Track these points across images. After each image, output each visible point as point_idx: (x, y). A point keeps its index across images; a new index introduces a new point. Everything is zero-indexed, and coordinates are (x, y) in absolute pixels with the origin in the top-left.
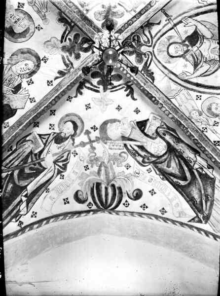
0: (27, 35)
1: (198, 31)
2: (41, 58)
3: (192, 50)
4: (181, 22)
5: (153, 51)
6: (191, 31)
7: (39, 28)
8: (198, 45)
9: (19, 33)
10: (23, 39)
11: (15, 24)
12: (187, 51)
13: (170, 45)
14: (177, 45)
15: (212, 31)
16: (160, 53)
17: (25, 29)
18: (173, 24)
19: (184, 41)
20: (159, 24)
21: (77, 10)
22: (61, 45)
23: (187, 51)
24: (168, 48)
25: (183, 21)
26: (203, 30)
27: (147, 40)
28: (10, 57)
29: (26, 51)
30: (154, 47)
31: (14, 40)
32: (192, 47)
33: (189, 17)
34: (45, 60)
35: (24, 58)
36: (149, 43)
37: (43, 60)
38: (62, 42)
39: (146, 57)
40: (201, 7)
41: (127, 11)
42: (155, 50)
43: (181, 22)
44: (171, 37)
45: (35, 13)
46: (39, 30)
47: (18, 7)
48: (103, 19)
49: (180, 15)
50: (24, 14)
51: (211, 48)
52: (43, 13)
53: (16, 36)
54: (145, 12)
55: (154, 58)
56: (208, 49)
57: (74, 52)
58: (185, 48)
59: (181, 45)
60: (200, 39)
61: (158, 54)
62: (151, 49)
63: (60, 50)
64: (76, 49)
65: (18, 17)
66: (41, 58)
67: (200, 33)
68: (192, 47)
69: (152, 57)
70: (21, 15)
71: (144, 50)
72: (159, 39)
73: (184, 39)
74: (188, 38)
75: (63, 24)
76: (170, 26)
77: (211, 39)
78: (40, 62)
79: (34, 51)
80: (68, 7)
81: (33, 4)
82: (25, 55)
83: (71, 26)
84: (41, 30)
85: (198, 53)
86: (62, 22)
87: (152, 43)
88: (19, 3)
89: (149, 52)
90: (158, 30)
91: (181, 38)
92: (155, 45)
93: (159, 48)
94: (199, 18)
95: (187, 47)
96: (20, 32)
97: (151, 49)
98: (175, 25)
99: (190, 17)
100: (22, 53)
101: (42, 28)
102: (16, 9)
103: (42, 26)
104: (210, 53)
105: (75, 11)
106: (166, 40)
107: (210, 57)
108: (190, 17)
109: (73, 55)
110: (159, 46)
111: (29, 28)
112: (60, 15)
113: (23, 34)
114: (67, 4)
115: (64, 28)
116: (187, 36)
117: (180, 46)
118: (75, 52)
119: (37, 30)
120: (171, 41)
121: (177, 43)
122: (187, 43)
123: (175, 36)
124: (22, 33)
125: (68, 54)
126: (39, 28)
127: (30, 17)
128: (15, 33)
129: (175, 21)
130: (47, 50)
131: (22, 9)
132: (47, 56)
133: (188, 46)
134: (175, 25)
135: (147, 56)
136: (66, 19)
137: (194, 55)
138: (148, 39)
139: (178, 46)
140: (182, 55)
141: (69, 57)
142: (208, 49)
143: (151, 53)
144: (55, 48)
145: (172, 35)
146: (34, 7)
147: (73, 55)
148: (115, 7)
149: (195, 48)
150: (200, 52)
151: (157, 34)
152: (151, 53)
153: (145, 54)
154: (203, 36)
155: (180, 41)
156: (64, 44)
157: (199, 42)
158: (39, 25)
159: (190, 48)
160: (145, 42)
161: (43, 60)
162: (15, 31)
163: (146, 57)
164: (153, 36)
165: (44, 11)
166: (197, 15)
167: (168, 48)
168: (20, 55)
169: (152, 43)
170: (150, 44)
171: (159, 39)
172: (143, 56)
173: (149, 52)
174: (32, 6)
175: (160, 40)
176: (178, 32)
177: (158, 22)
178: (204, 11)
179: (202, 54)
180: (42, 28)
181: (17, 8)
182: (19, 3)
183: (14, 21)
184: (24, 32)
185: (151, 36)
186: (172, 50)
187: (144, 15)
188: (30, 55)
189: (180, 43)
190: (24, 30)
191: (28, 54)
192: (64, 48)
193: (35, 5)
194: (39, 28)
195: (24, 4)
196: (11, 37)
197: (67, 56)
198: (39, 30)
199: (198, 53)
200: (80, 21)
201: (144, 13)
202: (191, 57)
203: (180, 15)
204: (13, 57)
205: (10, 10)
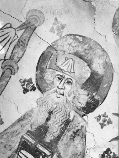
11: (74, 81)
47: (34, 89)
52: (20, 33)
65: (57, 83)
70: (49, 76)
81: (14, 64)
88: (25, 91)
102: (42, 92)
127: (43, 58)
131: (34, 81)
146: (16, 59)
162: (89, 76)
165: (12, 32)
174: (16, 63)
181: (37, 90)
182: (25, 91)
183: (68, 87)
190: (78, 60)
193: (11, 58)
195: (23, 82)
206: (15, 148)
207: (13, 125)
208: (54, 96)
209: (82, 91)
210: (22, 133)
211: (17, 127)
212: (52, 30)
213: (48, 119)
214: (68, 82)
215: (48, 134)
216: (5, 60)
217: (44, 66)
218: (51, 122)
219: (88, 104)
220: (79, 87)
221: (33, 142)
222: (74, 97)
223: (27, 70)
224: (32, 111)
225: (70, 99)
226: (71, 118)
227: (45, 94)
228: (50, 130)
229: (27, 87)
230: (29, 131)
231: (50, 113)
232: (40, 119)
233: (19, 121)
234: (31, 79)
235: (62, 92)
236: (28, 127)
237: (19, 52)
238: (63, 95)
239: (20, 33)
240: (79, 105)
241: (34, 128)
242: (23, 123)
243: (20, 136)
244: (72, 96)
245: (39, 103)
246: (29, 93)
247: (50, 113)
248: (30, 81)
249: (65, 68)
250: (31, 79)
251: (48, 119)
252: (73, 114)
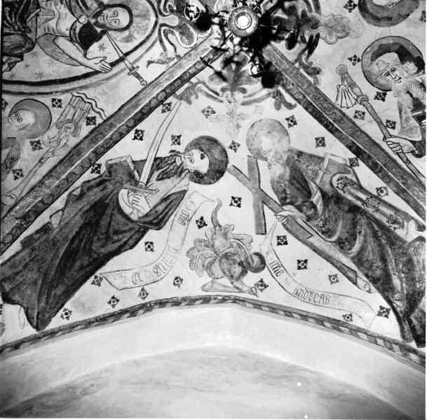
0: (376, 48)
1: (80, 48)
2: (357, 8)
3: (88, 17)
4: (113, 65)
5: (157, 16)
6: (94, 48)
7: (355, 59)
8: (79, 26)
9: (389, 52)
10: (384, 42)
12: (96, 15)
13: (127, 27)
14: (115, 25)
15: (58, 50)
16: (144, 13)
17: (379, 59)
18: (126, 62)
19: (104, 32)
20: (150, 63)
21: (288, 88)
22: (320, 28)
23: (96, 15)
24: (131, 22)
25: (109, 66)
26: (73, 50)
27: (170, 36)
28: (412, 12)
29: (383, 23)
30: (156, 23)
31: (403, 43)
32: (89, 22)
33: (100, 72)
34: (350, 5)
35: (387, 10)
36: (164, 31)
37: (355, 6)
38: (318, 36)
39: (169, 6)
40: (81, 88)
41: (204, 84)
42: (153, 19)
43: (113, 65)
44: (128, 39)
45: (358, 84)
46: (355, 56)
47: (385, 94)
48: (244, 71)
49: (116, 75)
50: (377, 83)
51: (54, 21)
52: (346, 83)
53: (397, 47)
54: (174, 81)
55: (156, 4)
56: (59, 18)
57: (297, 17)
58: (100, 20)
59: (108, 25)
60: (77, 36)
61: (148, 11)
62: (161, 20)
63: (321, 22)
64: (295, 22)
66: (357, 8)
67: (77, 45)
68: (89, 22)
69: (158, 6)
70: (382, 81)
71: (174, 19)
72: (148, 37)
73: (105, 38)
74: (97, 37)
75: (313, 66)
76: (131, 58)
77: (57, 36)
78: (359, 4)
79: (368, 22)
80: (303, 92)
82: (385, 15)
83: (300, 63)
84: (351, 55)
85: (78, 12)
86: (314, 69)
87: (160, 30)
88: (383, 100)
89: (164, 16)
90: (149, 53)
91: (109, 37)
92: (154, 28)
93: (147, 21)
94: (83, 70)
95: (97, 22)
96: (388, 54)
97: (161, 20)
98: (121, 60)
99: (97, 72)
100: (390, 19)
101: (350, 59)
102: (390, 90)
103: (349, 63)
104: (56, 12)
105: (291, 86)
106: (136, 35)
107: (56, 5)
108: (97, 72)
109: (300, 13)
110: (147, 25)
111: (372, 60)
112: (317, 81)
113: (382, 50)
114: (305, 97)
115: (311, 58)
116: (101, 42)
117: (110, 24)
118: (295, 18)
119: (359, 56)
120: (126, 33)
121: (115, 30)
122: (99, 30)
123: (121, 41)
124: (385, 52)
125: (308, 14)
126: (355, 59)
128: (396, 52)
129: (122, 65)
130: (345, 21)
131: (381, 92)
132: (346, 13)
133: (97, 24)
134: (121, 60)
135: (167, 7)
136: (308, 73)
137: (84, 8)
138: (167, 38)
139: (113, 23)
140: (104, 9)
141: (307, 9)
142: (59, 18)
143: (161, 13)
144: (331, 25)
145: (125, 44)
147: (300, 13)
148: (223, 90)
149: (83, 20)
150: (73, 14)
151: (152, 45)
152: (161, 13)
153: (172, 11)
154: (71, 40)
155: (110, 32)
156: (314, 32)
157: (78, 30)
158: (354, 64)
159: (93, 21)
160: (172, 33)
161: (355, 6)
162: (396, 55)
163: (169, 6)
164: (158, 42)
165: (342, 86)
166: (86, 76)
167: (131, 22)
168: (395, 15)
169: (160, 30)
170: (163, 28)
171: (148, 37)
172: (175, 9)
173: (164, 16)
175: (147, 34)
176: (116, 48)
177: (152, 65)
178: (72, 83)
179: (70, 10)
180: (350, 59)
181: (388, 93)
182: (383, 100)
184: (381, 54)
185: (161, 42)
186: (123, 18)
187: (176, 78)
188: (378, 15)
189: (110, 29)
191: (379, 15)
192: (315, 25)
193: (358, 97)
194: (355, 60)
195: (376, 98)
196: (406, 46)
197: (310, 10)
198: (355, 56)
199: (78, 12)
200: (284, 70)
201: (176, 80)
202: (89, 5)
203: (116, 75)
204: (407, 13)
205: (400, 89)
206: (417, 125)
207: (401, 118)
208: (397, 84)
209: (406, 65)
210: (409, 113)
211: (404, 116)
212: (354, 64)
213: (411, 96)
214: (393, 71)
215: (422, 101)
216: (357, 100)
217: (374, 80)
218: (414, 95)
219: (416, 65)
220: (401, 66)
221: (421, 112)
222: (407, 72)
223: (371, 92)
224: (399, 103)
225: (406, 75)
226: (421, 81)
227: (393, 89)
228: (420, 98)
229: (381, 96)
230: (412, 111)
231: (408, 92)
232: (407, 102)
233: (400, 112)
234: (377, 92)
235: (397, 78)
236: (409, 110)
237: (356, 90)
238: (400, 78)
239: (346, 83)
240: (415, 71)
241: (412, 107)
242: (403, 112)
243: (411, 118)
244: (405, 73)
245: (398, 94)
246: (386, 98)
247: (408, 92)
248: (378, 93)
249: (382, 68)
250: (377, 92)
251: (411, 96)
252: (418, 79)
